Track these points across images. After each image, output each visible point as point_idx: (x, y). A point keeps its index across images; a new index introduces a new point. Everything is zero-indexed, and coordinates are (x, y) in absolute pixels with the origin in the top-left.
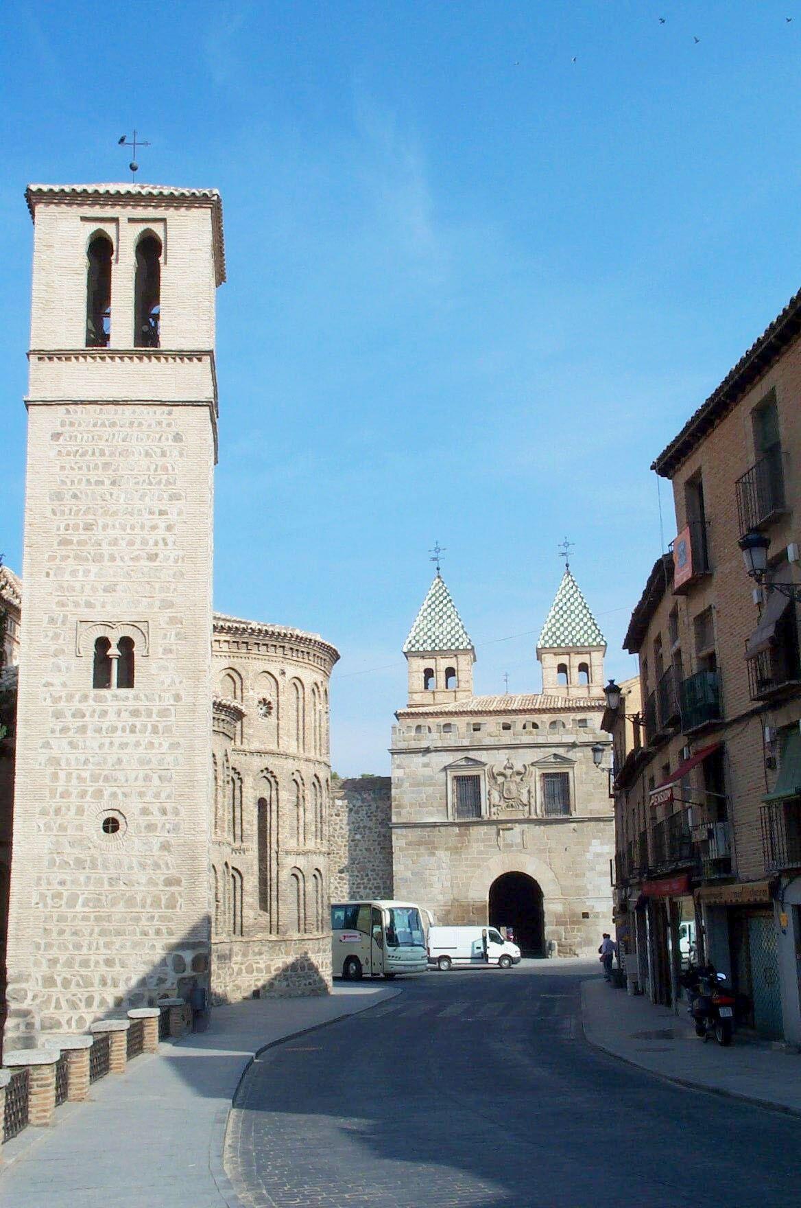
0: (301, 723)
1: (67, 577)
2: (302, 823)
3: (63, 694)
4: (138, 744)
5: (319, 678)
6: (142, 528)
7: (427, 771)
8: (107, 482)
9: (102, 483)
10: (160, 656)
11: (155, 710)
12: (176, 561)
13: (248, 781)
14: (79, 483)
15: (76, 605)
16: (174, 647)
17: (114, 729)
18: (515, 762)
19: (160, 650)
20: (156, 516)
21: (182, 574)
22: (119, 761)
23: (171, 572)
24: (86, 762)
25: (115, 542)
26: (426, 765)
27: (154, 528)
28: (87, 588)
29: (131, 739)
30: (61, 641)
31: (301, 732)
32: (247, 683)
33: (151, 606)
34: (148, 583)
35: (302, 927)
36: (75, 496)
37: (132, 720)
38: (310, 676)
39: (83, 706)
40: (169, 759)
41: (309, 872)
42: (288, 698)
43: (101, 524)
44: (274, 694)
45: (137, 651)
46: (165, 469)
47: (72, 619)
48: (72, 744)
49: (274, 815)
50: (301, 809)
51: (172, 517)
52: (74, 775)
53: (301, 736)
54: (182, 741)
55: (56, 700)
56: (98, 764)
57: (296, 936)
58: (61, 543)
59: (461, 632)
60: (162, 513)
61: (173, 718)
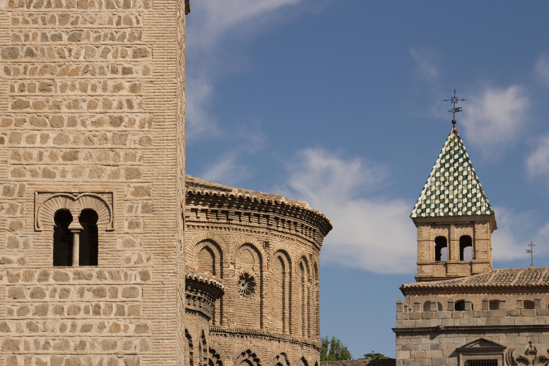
0: (287, 301)
1: (23, 144)
3: (22, 272)
4: (101, 327)
5: (306, 250)
6: (105, 89)
7: (437, 354)
8: (65, 37)
9: (60, 38)
10: (126, 230)
11: (120, 289)
12: (142, 126)
14: (34, 38)
15: (34, 174)
16: (141, 220)
17: (76, 310)
18: (538, 346)
19: (126, 224)
20: (120, 75)
21: (149, 140)
22: (82, 345)
23: (137, 138)
24: (47, 345)
25: (75, 104)
26: (435, 347)
27: (118, 88)
28: (46, 154)
29: (95, 321)
30: (18, 214)
31: (287, 312)
32: (228, 257)
33: (115, 175)
34: (112, 149)
36: (30, 53)
37: (95, 300)
38: (296, 249)
39: (42, 285)
40: (136, 342)
42: (273, 271)
43: (59, 84)
44: (257, 268)
45: (102, 225)
46: (130, 22)
47: (29, 190)
48: (31, 327)
51: (138, 75)
52: (34, 360)
53: (287, 315)
54: (149, 323)
55: (13, 278)
56: (59, 347)
58: (15, 106)
59: (479, 195)
60: (127, 71)
61: (139, 298)
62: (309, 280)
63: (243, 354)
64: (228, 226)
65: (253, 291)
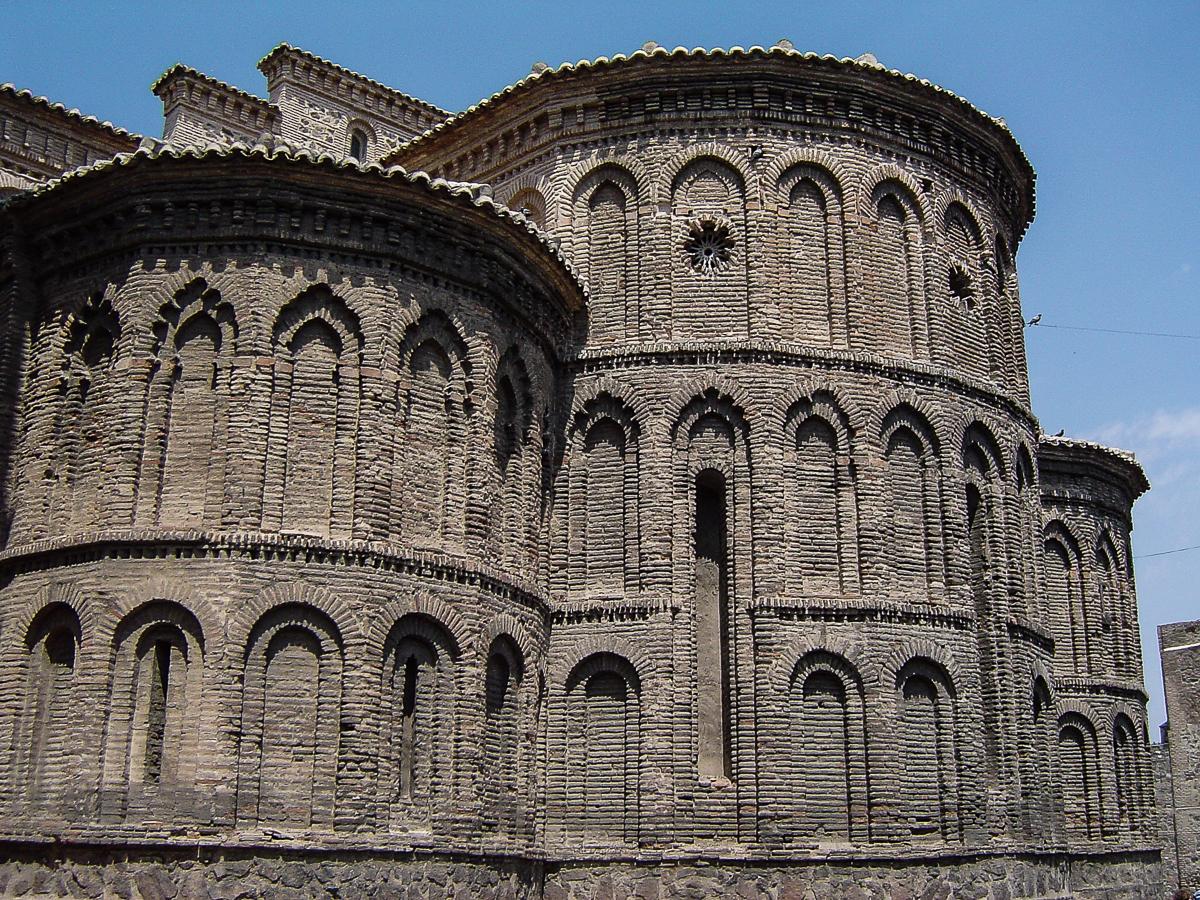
2: (850, 529)
13: (656, 427)
32: (654, 190)
35: (860, 823)
41: (882, 673)
49: (742, 511)
50: (848, 497)
53: (839, 305)
57: (829, 846)
62: (927, 237)
63: (696, 401)
64: (650, 127)
65: (725, 258)
